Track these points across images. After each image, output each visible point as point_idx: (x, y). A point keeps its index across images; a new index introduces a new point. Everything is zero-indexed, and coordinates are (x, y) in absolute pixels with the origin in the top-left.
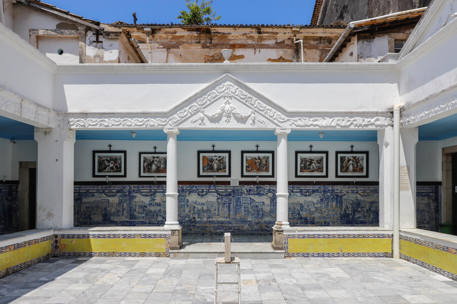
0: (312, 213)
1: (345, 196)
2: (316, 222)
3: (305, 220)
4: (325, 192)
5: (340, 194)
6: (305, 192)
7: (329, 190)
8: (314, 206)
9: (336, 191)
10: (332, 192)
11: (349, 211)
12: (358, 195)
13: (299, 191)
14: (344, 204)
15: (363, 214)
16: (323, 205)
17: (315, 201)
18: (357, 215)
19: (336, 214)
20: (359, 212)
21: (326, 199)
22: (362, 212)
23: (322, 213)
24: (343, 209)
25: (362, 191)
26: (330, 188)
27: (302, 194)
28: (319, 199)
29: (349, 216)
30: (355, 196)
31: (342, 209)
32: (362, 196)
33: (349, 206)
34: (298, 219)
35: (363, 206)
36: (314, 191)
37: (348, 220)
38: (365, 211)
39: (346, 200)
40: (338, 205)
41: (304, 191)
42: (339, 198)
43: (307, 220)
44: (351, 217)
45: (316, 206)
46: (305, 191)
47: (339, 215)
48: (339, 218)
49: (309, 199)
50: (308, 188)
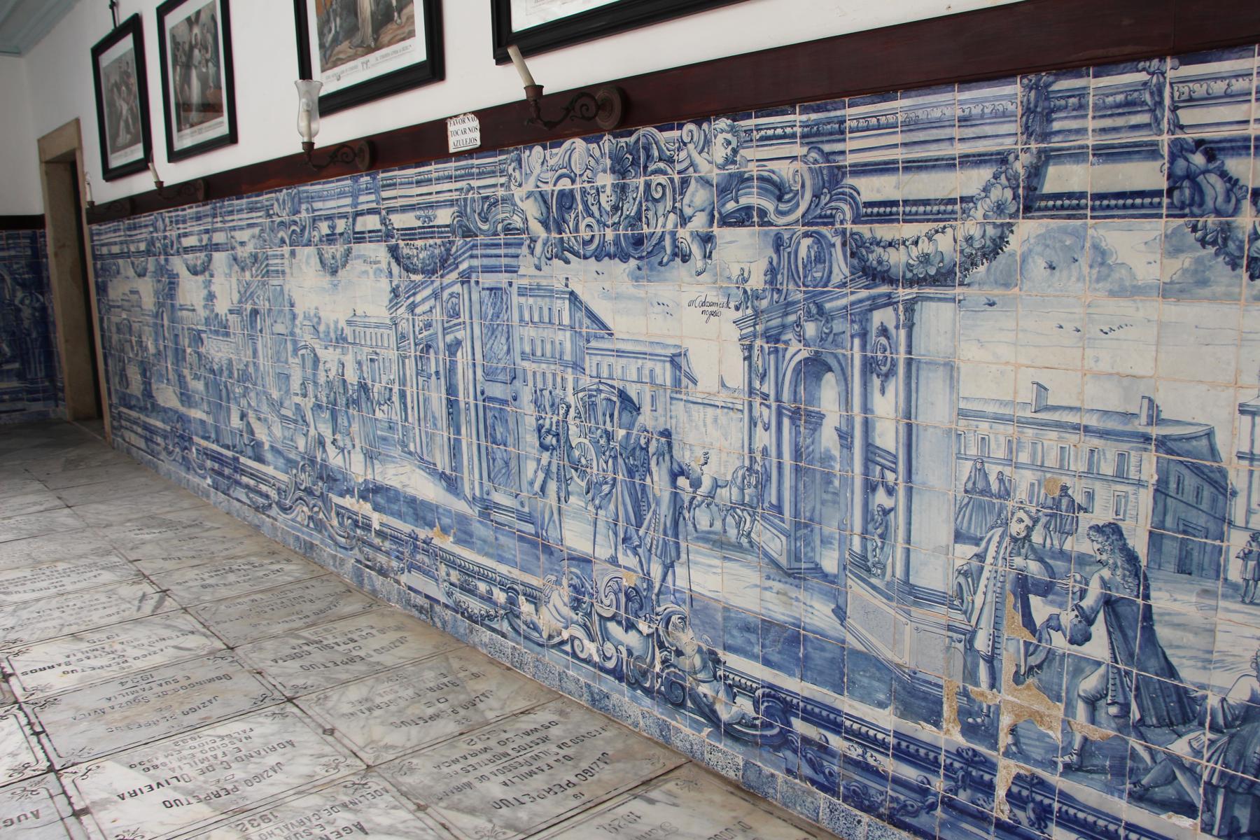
13: (1147, 175)
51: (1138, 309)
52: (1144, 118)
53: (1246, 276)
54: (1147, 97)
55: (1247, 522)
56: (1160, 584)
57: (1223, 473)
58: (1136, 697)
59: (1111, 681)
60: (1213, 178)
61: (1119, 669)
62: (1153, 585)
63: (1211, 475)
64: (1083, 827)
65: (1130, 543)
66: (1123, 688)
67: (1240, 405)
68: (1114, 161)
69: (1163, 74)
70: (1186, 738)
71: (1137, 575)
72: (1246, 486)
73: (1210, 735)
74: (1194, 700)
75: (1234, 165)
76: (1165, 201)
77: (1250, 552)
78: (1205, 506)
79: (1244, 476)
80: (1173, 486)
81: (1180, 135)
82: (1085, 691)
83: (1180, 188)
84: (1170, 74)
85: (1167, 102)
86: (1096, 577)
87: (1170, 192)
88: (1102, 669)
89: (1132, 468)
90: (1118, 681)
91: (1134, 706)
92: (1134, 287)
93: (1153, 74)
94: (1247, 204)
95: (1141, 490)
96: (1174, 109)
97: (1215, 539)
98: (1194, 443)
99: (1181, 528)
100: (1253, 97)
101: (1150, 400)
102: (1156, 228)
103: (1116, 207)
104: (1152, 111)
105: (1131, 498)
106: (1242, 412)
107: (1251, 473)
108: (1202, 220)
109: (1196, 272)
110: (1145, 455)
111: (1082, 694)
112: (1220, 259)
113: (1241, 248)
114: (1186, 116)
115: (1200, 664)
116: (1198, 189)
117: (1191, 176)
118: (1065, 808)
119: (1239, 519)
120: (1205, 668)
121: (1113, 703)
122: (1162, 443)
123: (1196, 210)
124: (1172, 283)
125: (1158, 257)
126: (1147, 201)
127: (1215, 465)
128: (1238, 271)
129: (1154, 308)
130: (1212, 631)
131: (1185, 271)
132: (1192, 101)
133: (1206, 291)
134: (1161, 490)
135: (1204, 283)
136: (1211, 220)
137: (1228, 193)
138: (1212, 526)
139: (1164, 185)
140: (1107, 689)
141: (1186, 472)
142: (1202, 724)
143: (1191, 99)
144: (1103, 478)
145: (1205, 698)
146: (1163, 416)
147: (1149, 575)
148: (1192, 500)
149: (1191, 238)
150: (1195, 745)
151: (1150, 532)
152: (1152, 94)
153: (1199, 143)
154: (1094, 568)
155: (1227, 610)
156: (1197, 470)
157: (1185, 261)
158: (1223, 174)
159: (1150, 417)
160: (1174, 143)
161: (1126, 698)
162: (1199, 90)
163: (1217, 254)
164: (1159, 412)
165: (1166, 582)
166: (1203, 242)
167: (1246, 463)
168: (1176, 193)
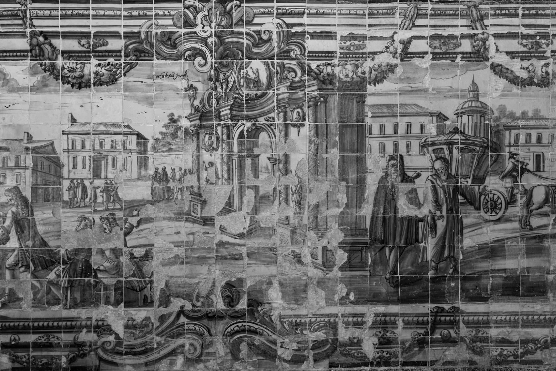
0: (124, 216)
1: (386, 85)
2: (159, 286)
3: (72, 272)
4: (228, 54)
5: (342, 71)
6: (68, 54)
7: (259, 40)
8: (143, 163)
9: (312, 45)
10: (285, 54)
11: (414, 200)
12: (483, 76)
13: (22, 44)
14: (373, 143)
15: (525, 224)
16: (217, 157)
17: (151, 125)
18: (479, 232)
19: (318, 227)
20: (494, 206)
21: (237, 105)
22: (517, 210)
23: (208, 221)
24: (372, 183)
25: (514, 45)
26: (270, 24)
27: (52, 70)
28: (182, 109)
29: (412, 240)
30: (461, 79)
31: (361, 182)
32: (514, 80)
33: (417, 160)
34: (22, 262)
35: (526, 156)
36: (140, 50)
37: (407, 266)
38: (539, 196)
39: (390, 111)
40: (334, 154)
41: (61, 44)
42: (334, 101)
43: (88, 270)
44: (430, 245)
45: (159, 161)
46: (73, 45)
47: (335, 236)
48: (342, 257)
49: (106, 107)
50: (92, 25)
51: (20, 97)
52: (20, 22)
53: (61, 83)
54: (20, 13)
55: (69, 176)
56: (37, 209)
57: (58, 158)
58: (32, 260)
59: (20, 257)
60: (47, 46)
61: (23, 250)
62: (34, 209)
63: (54, 160)
64: (13, 329)
65: (24, 194)
66: (26, 257)
67: (63, 131)
68: (8, 38)
69: (26, 5)
70: (54, 271)
71: (27, 207)
72: (67, 163)
73: (63, 267)
74: (56, 253)
75: (54, 42)
76: (29, 54)
77: (71, 187)
78: (53, 172)
79: (66, 158)
80: (39, 167)
81: (34, 29)
82: (9, 265)
83: (35, 49)
84: (29, 6)
85: (28, 16)
86: (10, 212)
87: (31, 51)
88: (16, 253)
89: (22, 162)
90: (23, 256)
91: (31, 264)
92: (18, 88)
93: (22, 5)
94: (60, 56)
95: (27, 171)
96: (31, 19)
97: (57, 185)
98: (47, 148)
99: (44, 183)
100: (59, 17)
101: (28, 133)
102: (28, 63)
103: (10, 56)
104: (23, 19)
105: (23, 174)
106: (63, 134)
107: (69, 157)
108: (44, 62)
109: (42, 81)
110: (27, 156)
111: (7, 266)
112: (52, 76)
113: (59, 73)
114: (36, 22)
115: (56, 238)
116: (41, 50)
117: (39, 45)
118: (4, 324)
119: (66, 176)
120: (58, 239)
121: (22, 266)
122: (34, 150)
123: (41, 58)
124: (34, 86)
125: (27, 76)
126: (22, 54)
127: (55, 155)
128: (58, 81)
129: (29, 96)
130: (59, 223)
131: (38, 81)
132: (38, 17)
133: (47, 89)
134: (35, 170)
135: (46, 86)
136: (47, 62)
137: (53, 52)
138: (55, 179)
139: (29, 48)
140: (19, 261)
141: (43, 159)
142: (59, 263)
143: (37, 16)
144: (11, 169)
145: (59, 251)
146: (33, 139)
147: (33, 205)
148: (47, 171)
149: (40, 69)
150: (57, 273)
151: (32, 188)
152: (22, 12)
153: (41, 33)
154: (9, 208)
155: (64, 212)
156: (48, 159)
157: (38, 77)
158: (51, 45)
159: (28, 140)
160: (31, 32)
161: (27, 262)
162: (40, 13)
163: (50, 75)
164: (32, 137)
165: (39, 207)
166: (45, 70)
167: (66, 153)
168: (33, 51)
